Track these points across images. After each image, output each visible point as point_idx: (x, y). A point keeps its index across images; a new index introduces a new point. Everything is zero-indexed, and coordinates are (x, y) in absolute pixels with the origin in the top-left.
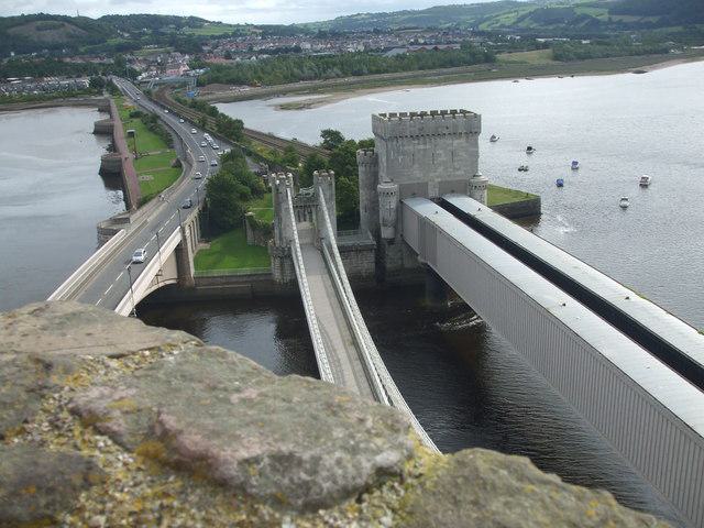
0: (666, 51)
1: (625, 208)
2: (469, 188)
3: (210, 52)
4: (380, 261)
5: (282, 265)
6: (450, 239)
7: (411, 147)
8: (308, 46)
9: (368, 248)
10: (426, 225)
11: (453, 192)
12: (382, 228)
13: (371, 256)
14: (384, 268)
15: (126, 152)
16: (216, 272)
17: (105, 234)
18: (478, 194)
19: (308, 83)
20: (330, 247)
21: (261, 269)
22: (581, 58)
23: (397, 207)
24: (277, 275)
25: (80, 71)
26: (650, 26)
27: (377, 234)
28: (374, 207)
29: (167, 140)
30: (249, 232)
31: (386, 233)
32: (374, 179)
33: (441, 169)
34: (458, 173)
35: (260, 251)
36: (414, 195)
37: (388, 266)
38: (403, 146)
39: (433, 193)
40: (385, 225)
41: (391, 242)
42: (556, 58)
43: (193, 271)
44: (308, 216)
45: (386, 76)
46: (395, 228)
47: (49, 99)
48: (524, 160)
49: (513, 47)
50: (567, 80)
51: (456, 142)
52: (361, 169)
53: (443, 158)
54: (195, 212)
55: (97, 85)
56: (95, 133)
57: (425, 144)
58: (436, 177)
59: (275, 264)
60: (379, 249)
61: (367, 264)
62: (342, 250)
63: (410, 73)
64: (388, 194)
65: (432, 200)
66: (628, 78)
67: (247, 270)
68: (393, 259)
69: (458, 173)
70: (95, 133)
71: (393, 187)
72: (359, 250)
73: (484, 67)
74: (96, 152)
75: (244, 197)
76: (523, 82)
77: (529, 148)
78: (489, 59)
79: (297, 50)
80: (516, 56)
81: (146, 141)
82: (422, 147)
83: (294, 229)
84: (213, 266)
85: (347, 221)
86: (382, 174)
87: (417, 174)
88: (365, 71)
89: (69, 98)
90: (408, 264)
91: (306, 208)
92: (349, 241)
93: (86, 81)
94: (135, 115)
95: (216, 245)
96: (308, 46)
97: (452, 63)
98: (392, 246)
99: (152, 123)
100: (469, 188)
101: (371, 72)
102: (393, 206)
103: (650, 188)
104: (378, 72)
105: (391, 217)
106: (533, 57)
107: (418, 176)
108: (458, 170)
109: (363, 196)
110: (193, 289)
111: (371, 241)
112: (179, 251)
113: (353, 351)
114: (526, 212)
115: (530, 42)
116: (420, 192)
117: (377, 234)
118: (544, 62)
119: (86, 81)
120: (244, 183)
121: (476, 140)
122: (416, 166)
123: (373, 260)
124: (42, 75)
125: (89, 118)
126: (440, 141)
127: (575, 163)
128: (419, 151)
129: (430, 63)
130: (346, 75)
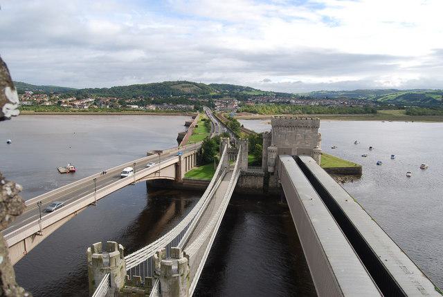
1: (409, 176)
2: (311, 153)
4: (266, 182)
8: (294, 101)
9: (261, 175)
14: (268, 185)
16: (192, 178)
17: (149, 155)
18: (315, 156)
22: (419, 114)
25: (192, 103)
27: (266, 170)
36: (285, 154)
37: (270, 185)
41: (273, 174)
42: (407, 114)
43: (183, 176)
45: (322, 115)
47: (176, 112)
49: (389, 108)
50: (410, 123)
51: (307, 131)
52: (264, 140)
55: (196, 109)
58: (296, 146)
60: (267, 176)
63: (334, 115)
73: (372, 115)
76: (387, 123)
77: (371, 148)
78: (374, 112)
79: (289, 103)
80: (387, 112)
82: (290, 131)
87: (287, 144)
88: (313, 112)
89: (184, 112)
91: (232, 154)
93: (192, 107)
95: (201, 168)
96: (294, 101)
97: (355, 113)
101: (316, 113)
102: (274, 157)
103: (427, 170)
104: (319, 113)
105: (272, 162)
106: (396, 112)
110: (181, 184)
112: (177, 166)
114: (350, 173)
115: (400, 107)
116: (287, 152)
117: (266, 170)
119: (192, 107)
126: (299, 130)
127: (393, 156)
129: (344, 111)
130: (303, 113)
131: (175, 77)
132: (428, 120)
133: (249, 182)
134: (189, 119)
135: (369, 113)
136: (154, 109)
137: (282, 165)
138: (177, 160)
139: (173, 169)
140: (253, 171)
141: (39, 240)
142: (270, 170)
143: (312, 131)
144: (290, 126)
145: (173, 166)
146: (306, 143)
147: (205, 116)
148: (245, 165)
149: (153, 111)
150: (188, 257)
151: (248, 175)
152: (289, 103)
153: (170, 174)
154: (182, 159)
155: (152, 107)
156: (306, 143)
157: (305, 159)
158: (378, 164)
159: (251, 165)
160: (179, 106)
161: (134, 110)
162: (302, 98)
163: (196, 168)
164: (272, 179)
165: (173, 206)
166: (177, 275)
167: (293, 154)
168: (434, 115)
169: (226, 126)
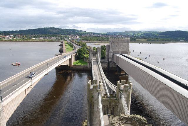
0: (169, 41)
1: (159, 62)
4: (108, 66)
5: (89, 64)
6: (122, 59)
9: (106, 63)
10: (118, 57)
13: (107, 64)
15: (64, 47)
16: (77, 65)
17: (56, 55)
19: (99, 41)
20: (99, 61)
21: (86, 65)
22: (152, 41)
24: (88, 66)
26: (166, 37)
27: (108, 60)
28: (108, 55)
29: (72, 47)
30: (84, 59)
31: (110, 60)
32: (108, 51)
35: (86, 62)
37: (110, 66)
41: (111, 62)
42: (148, 40)
43: (72, 64)
48: (139, 54)
49: (140, 38)
50: (150, 44)
54: (74, 54)
55: (61, 39)
56: (60, 45)
58: (120, 50)
59: (88, 64)
60: (109, 63)
61: (106, 66)
62: (101, 62)
64: (111, 52)
66: (162, 44)
67: (83, 65)
68: (111, 65)
70: (60, 45)
71: (112, 51)
72: (104, 63)
73: (134, 41)
74: (59, 48)
75: (84, 53)
76: (141, 44)
77: (140, 53)
78: (135, 40)
79: (99, 36)
80: (140, 40)
81: (68, 46)
83: (93, 58)
84: (77, 64)
85: (103, 58)
86: (110, 49)
87: (117, 49)
89: (57, 41)
90: (114, 66)
92: (103, 61)
93: (60, 38)
94: (68, 43)
95: (78, 61)
99: (70, 44)
105: (111, 57)
106: (143, 40)
109: (106, 53)
111: (107, 61)
112: (70, 60)
113: (100, 76)
115: (144, 38)
117: (108, 60)
118: (145, 41)
119: (60, 38)
120: (84, 51)
123: (107, 65)
124: (52, 37)
125: (60, 43)
126: (122, 43)
131: (52, 26)
132: (156, 43)
135: (133, 40)
136: (43, 39)
138: (70, 57)
139: (69, 61)
141: (30, 89)
144: (118, 42)
147: (67, 42)
149: (43, 40)
152: (99, 36)
153: (68, 63)
154: (72, 57)
155: (42, 38)
158: (146, 58)
160: (54, 38)
161: (33, 40)
162: (104, 35)
163: (76, 61)
165: (69, 77)
167: (120, 53)
168: (158, 41)
169: (79, 45)
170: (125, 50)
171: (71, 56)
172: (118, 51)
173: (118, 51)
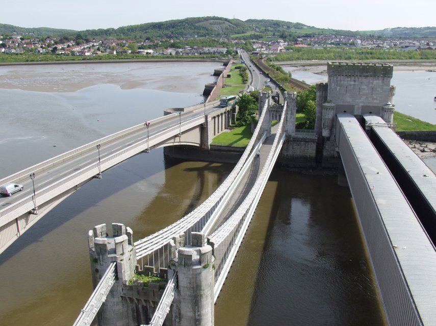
2: (382, 111)
3: (301, 41)
4: (319, 150)
7: (345, 83)
8: (359, 42)
9: (312, 141)
11: (371, 113)
12: (323, 130)
17: (166, 113)
23: (333, 118)
33: (363, 98)
34: (375, 101)
37: (325, 154)
38: (340, 81)
39: (358, 112)
40: (324, 128)
41: (328, 139)
44: (278, 117)
46: (331, 131)
51: (375, 82)
53: (366, 91)
57: (355, 81)
58: (360, 103)
60: (321, 143)
65: (356, 116)
69: (375, 101)
82: (352, 83)
87: (348, 99)
89: (212, 58)
91: (275, 112)
93: (225, 50)
98: (329, 142)
100: (382, 111)
102: (330, 117)
105: (328, 123)
107: (348, 100)
108: (376, 99)
112: (203, 128)
116: (348, 111)
117: (320, 134)
121: (389, 82)
122: (348, 94)
126: (365, 80)
128: (350, 85)
133: (297, 150)
134: (219, 66)
137: (341, 126)
138: (202, 121)
139: (197, 132)
140: (301, 135)
141: (33, 220)
142: (325, 133)
143: (383, 82)
145: (197, 131)
146: (373, 99)
148: (291, 128)
150: (212, 244)
151: (296, 140)
152: (353, 44)
153: (193, 139)
154: (209, 119)
156: (373, 99)
157: (373, 120)
159: (300, 127)
160: (206, 49)
164: (327, 146)
166: (199, 267)
167: (355, 114)
170: (377, 103)
171: (206, 117)
172: (353, 107)
173: (353, 107)
